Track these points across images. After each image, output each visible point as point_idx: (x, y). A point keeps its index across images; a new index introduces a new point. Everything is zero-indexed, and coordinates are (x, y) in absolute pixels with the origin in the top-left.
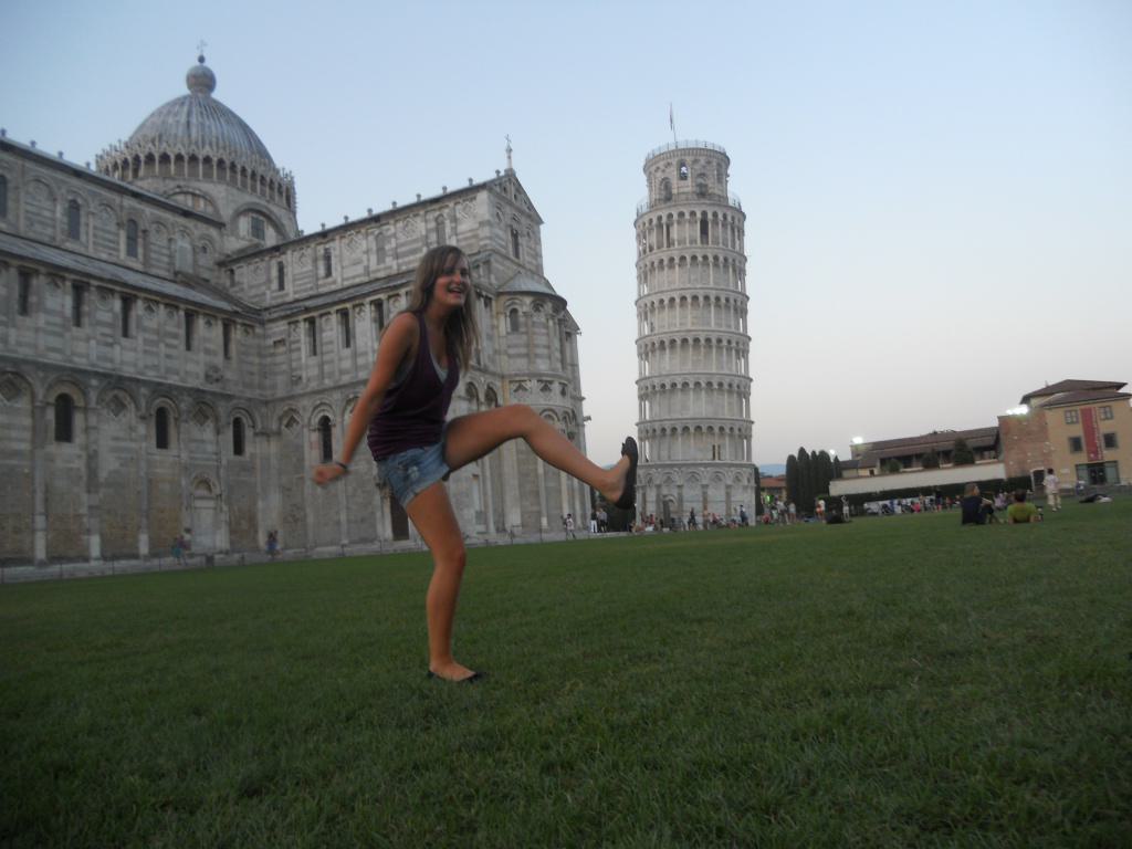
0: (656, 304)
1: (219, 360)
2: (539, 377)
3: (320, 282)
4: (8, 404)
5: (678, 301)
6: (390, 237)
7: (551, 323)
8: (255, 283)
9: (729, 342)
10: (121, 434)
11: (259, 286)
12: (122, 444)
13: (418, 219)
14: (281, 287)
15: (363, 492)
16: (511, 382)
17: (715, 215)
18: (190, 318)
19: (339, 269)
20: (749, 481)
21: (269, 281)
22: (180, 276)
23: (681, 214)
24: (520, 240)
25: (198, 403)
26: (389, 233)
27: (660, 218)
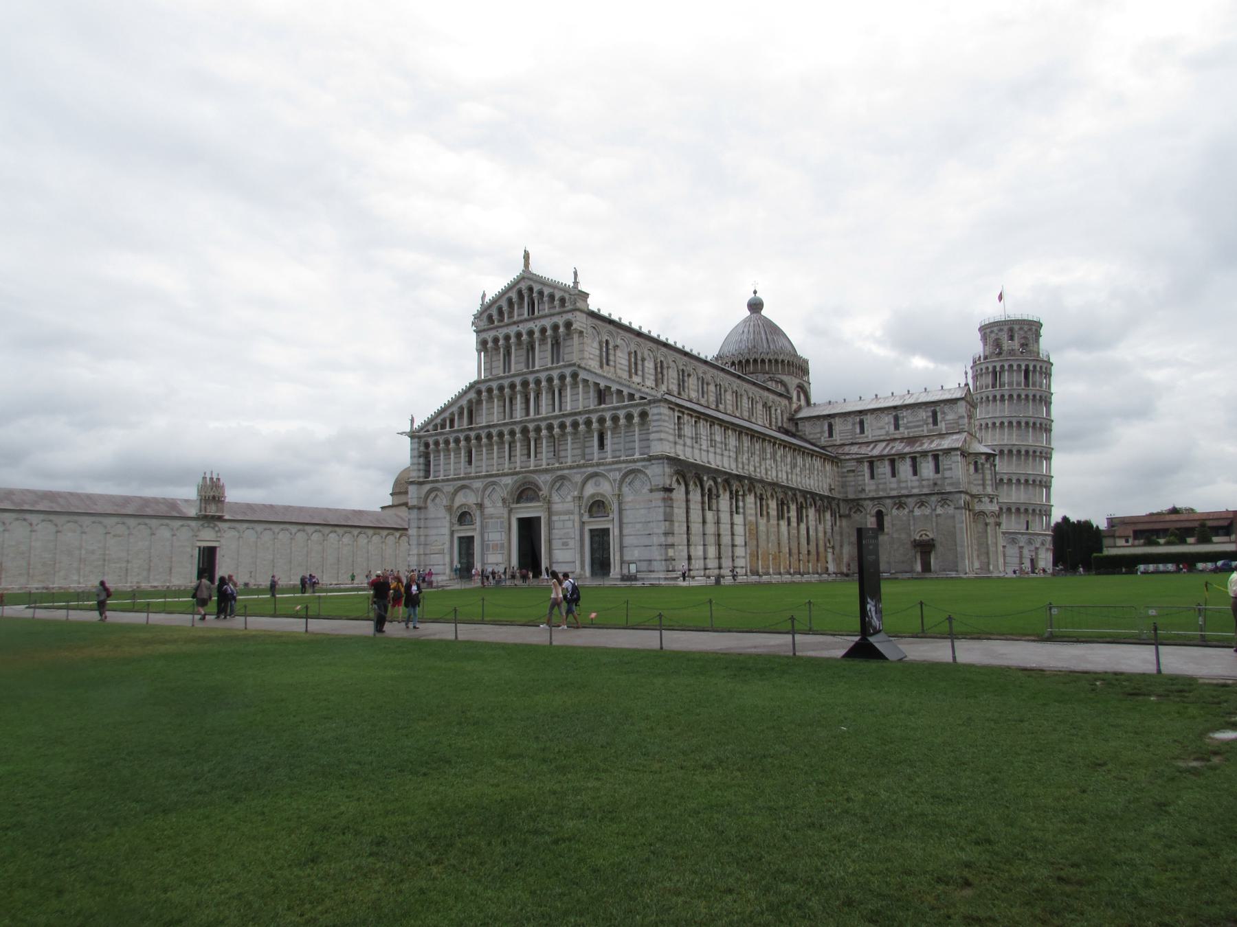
0: (990, 425)
2: (988, 496)
3: (857, 436)
5: (1006, 424)
6: (903, 417)
7: (993, 468)
8: (813, 431)
11: (815, 434)
13: (921, 410)
14: (831, 435)
17: (1035, 367)
18: (825, 459)
19: (870, 430)
20: (1050, 545)
21: (823, 432)
23: (1011, 366)
26: (902, 415)
27: (994, 367)
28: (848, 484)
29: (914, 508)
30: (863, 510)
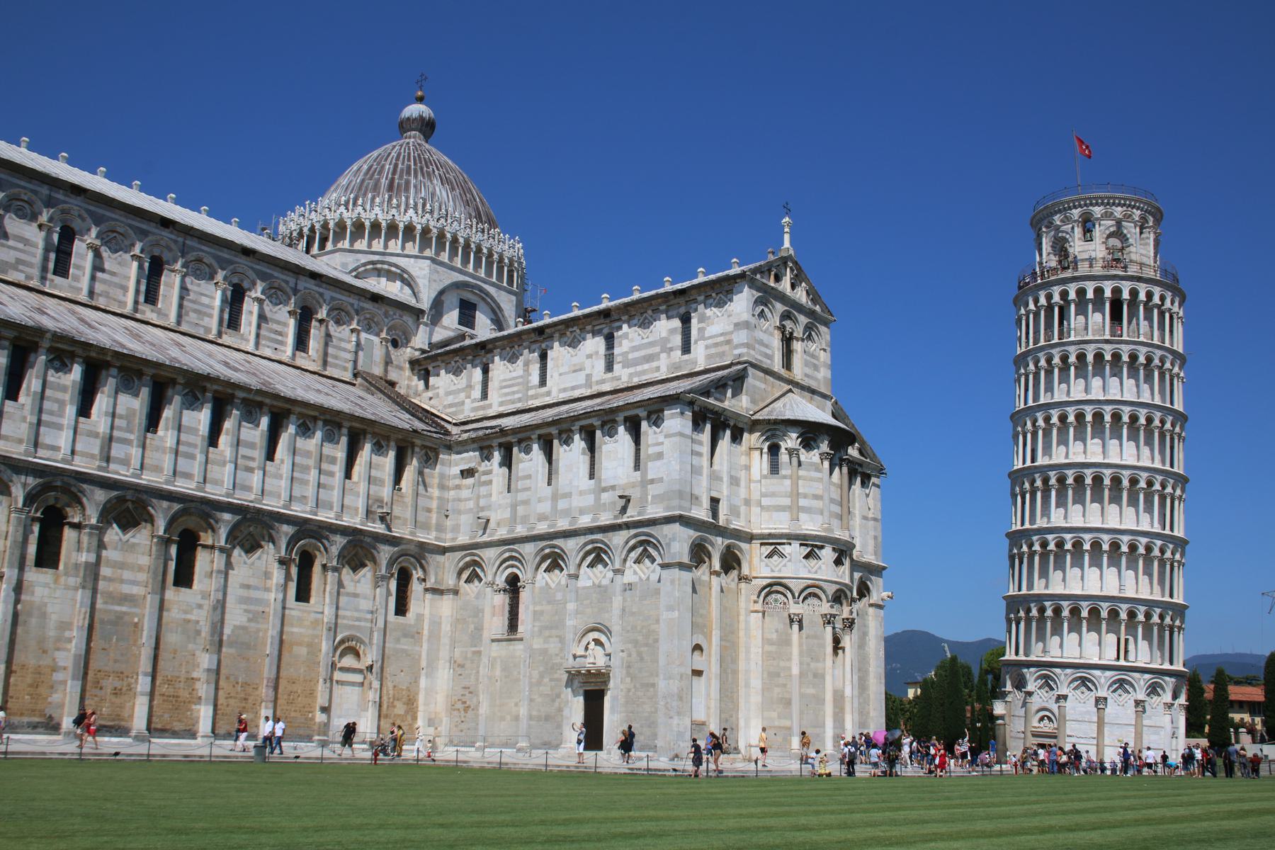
0: (1041, 423)
1: (386, 492)
2: (803, 539)
3: (531, 393)
4: (125, 538)
6: (621, 337)
7: (826, 464)
8: (454, 388)
9: (1150, 484)
10: (252, 582)
11: (459, 391)
12: (254, 594)
14: (485, 395)
15: (551, 680)
16: (762, 544)
17: (1134, 293)
19: (556, 375)
20: (1175, 697)
21: (470, 386)
22: (359, 380)
24: (797, 346)
25: (355, 546)
27: (1049, 297)
28: (462, 506)
29: (580, 565)
30: (482, 575)
